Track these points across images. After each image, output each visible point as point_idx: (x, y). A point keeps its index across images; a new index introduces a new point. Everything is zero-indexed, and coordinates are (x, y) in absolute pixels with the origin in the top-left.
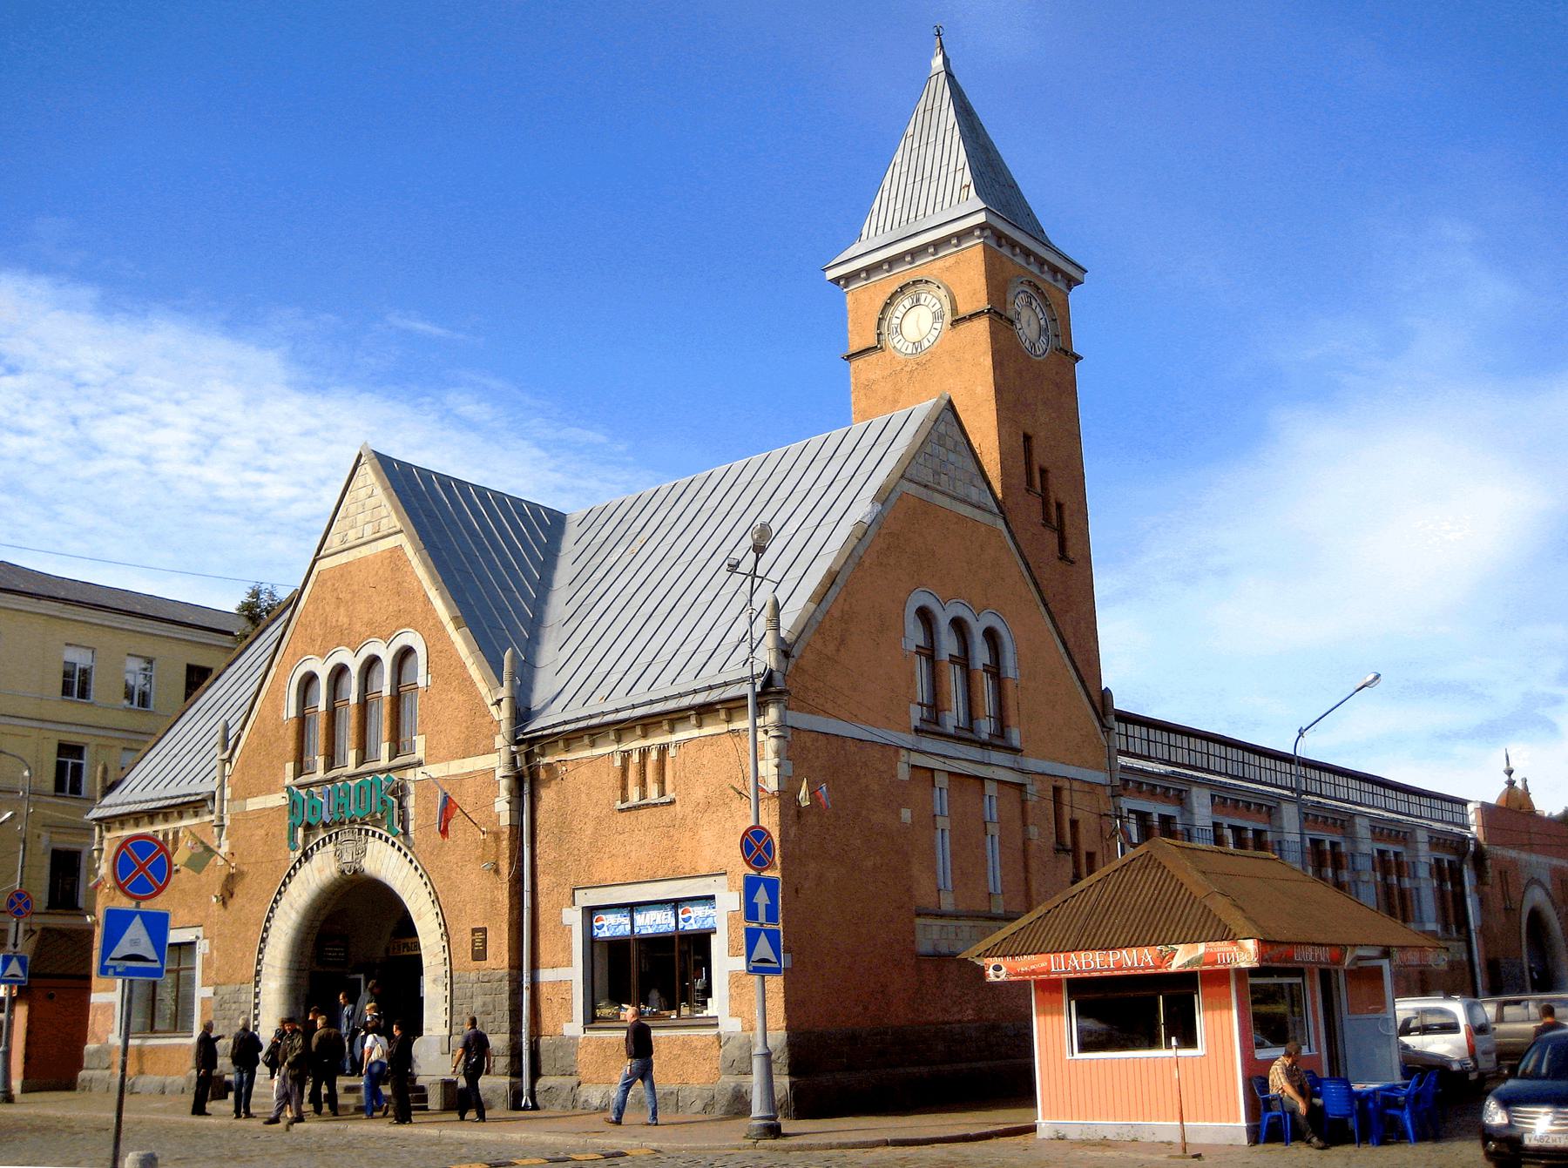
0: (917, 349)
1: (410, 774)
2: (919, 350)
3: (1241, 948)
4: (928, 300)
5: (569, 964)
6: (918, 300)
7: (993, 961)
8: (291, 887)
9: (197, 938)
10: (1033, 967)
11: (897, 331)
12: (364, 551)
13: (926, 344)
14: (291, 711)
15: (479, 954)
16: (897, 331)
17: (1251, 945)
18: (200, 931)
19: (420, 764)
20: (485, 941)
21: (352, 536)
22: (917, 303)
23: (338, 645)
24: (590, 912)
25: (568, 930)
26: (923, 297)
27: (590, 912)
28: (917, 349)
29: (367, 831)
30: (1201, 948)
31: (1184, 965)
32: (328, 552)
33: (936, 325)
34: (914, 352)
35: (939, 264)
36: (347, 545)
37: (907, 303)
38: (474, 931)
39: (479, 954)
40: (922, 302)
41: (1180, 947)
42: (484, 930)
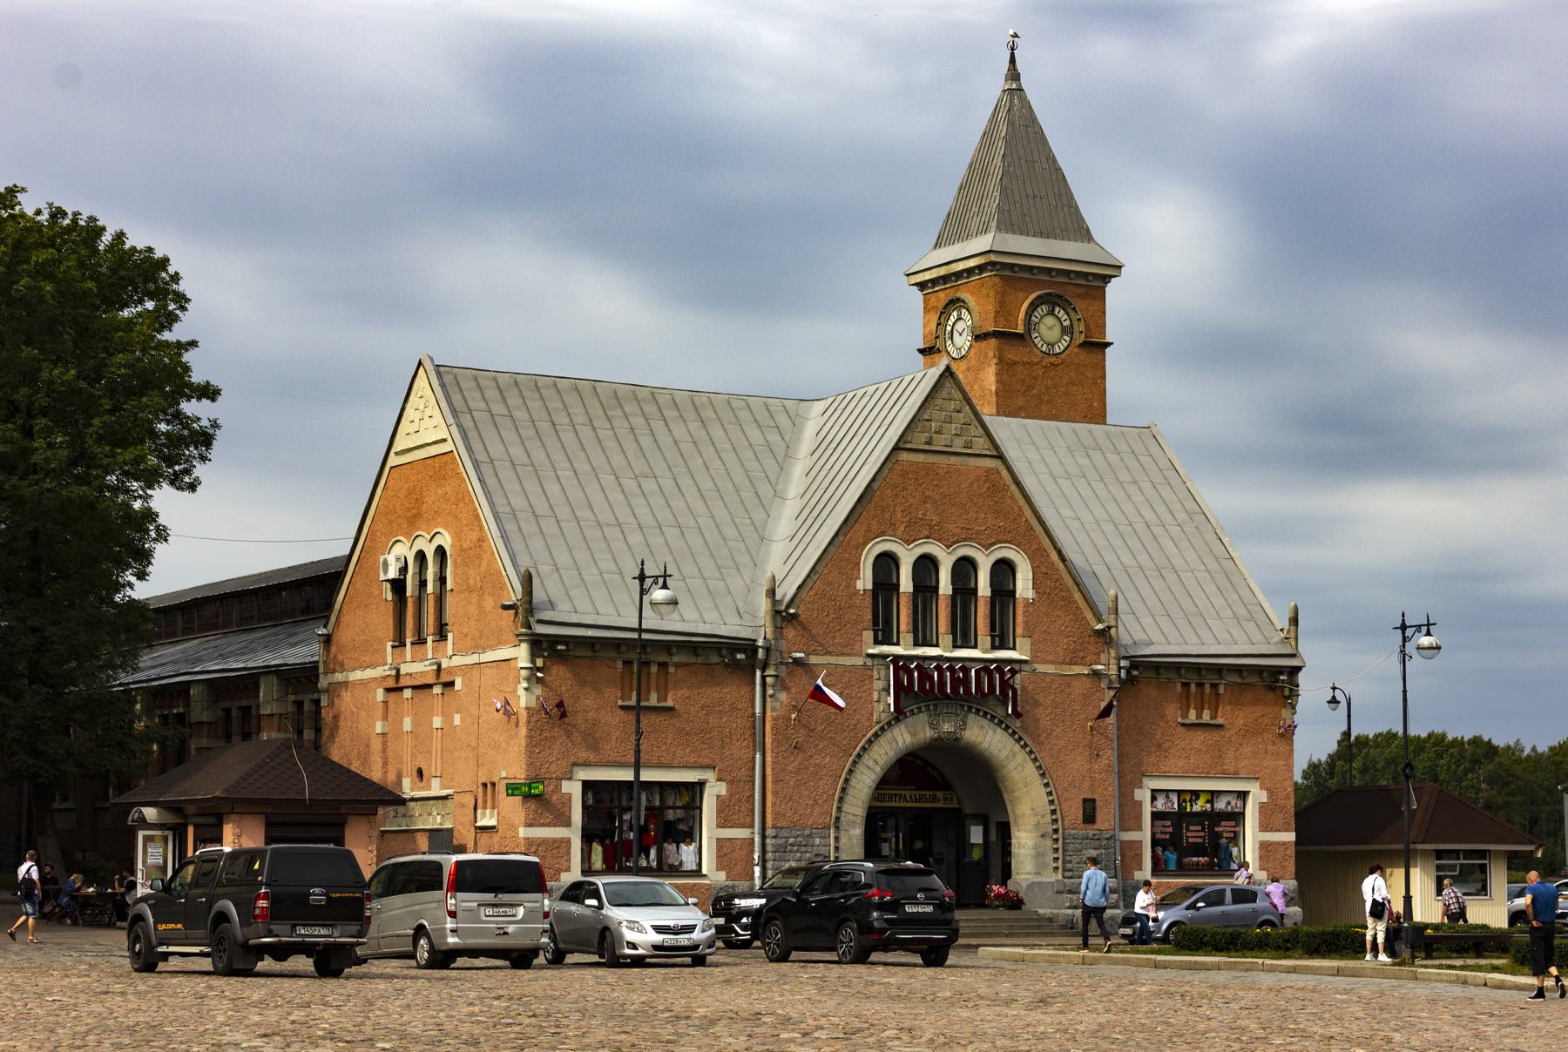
5: (1139, 828)
6: (1053, 310)
8: (875, 747)
12: (953, 459)
14: (865, 581)
15: (1089, 817)
18: (709, 776)
20: (1094, 809)
21: (940, 443)
22: (1051, 313)
23: (927, 537)
24: (1155, 794)
25: (1139, 804)
26: (1057, 309)
27: (1155, 794)
29: (970, 708)
32: (909, 446)
35: (1073, 289)
36: (932, 448)
38: (1085, 801)
39: (1089, 817)
42: (1093, 801)
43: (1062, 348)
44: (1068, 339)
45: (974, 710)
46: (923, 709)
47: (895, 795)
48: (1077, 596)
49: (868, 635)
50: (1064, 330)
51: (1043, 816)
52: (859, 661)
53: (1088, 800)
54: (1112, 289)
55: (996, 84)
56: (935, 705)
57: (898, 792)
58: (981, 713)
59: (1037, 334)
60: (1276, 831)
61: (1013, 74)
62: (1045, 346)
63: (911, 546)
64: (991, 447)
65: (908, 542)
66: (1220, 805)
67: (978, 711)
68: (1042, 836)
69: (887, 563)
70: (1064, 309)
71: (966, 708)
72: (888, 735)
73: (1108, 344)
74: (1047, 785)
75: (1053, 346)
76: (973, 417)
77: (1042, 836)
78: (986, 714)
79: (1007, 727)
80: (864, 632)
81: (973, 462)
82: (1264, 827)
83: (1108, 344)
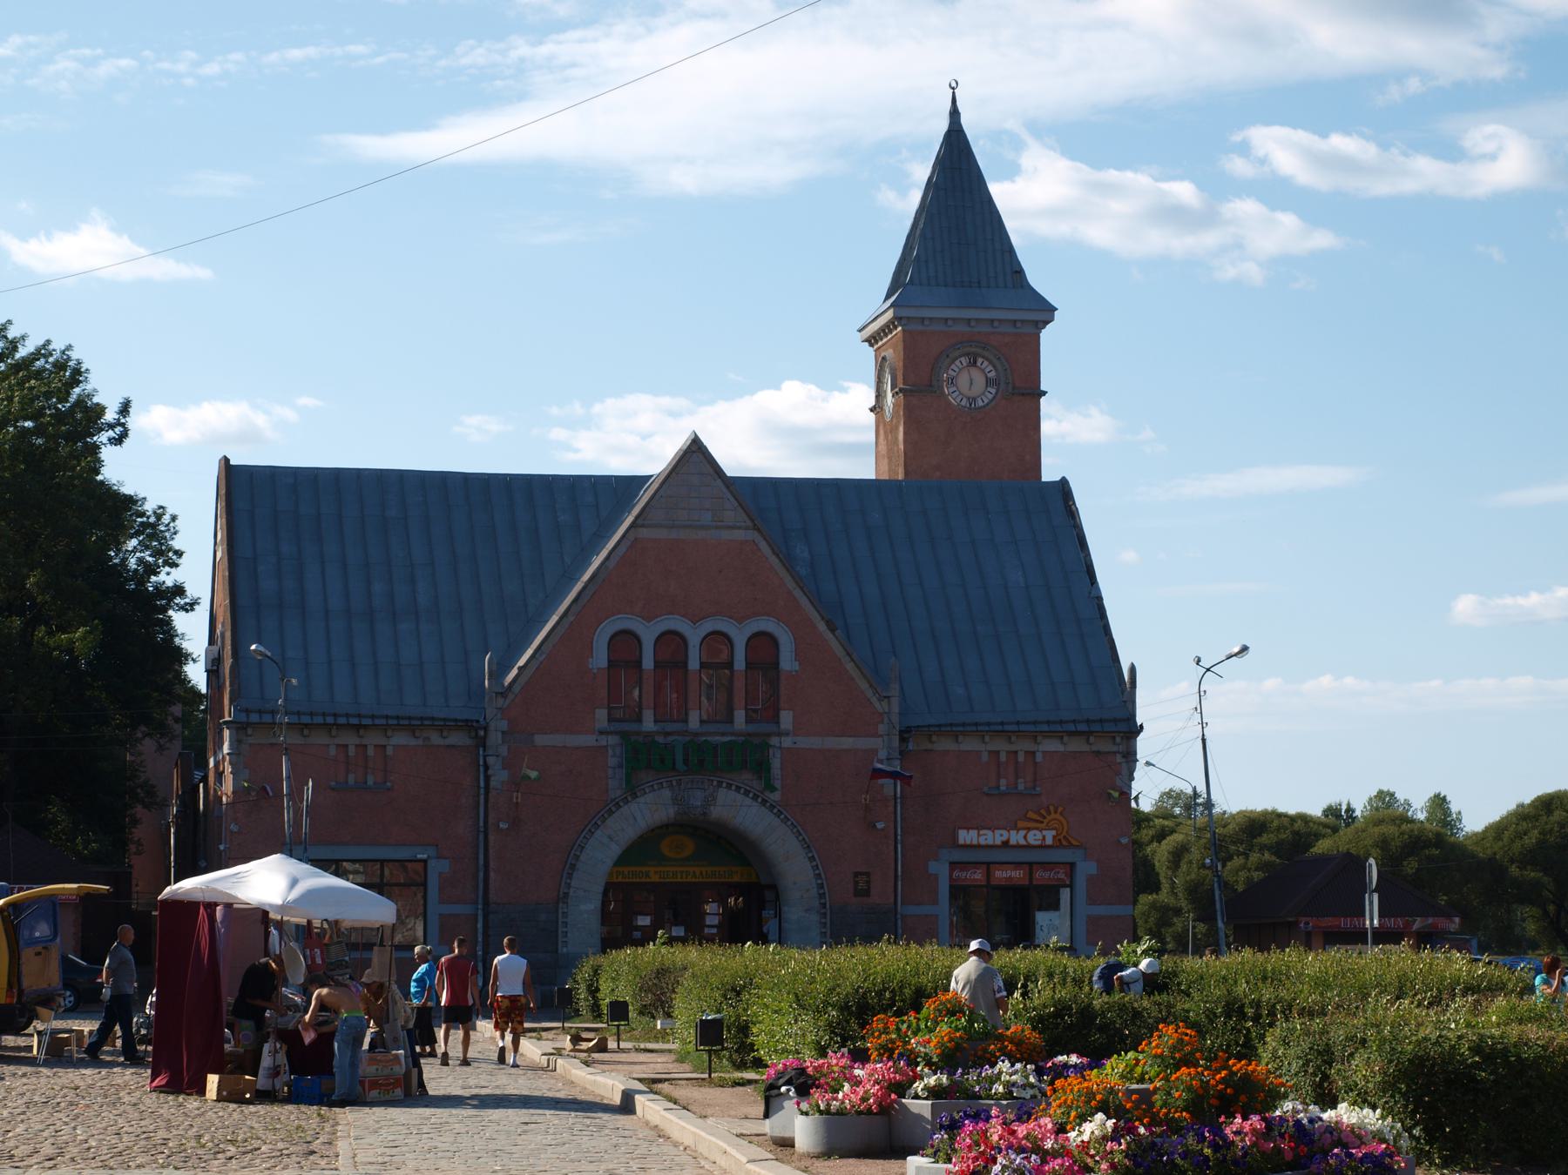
0: (970, 405)
1: (774, 741)
2: (973, 405)
3: (1454, 923)
4: (983, 366)
5: (935, 902)
6: (975, 362)
7: (1304, 920)
8: (609, 822)
9: (429, 856)
10: (1330, 924)
11: (952, 383)
13: (980, 403)
14: (600, 658)
16: (952, 383)
17: (1457, 920)
19: (787, 734)
20: (868, 882)
25: (936, 877)
26: (980, 361)
28: (970, 405)
30: (1430, 920)
31: (1419, 929)
33: (989, 389)
34: (968, 405)
37: (964, 360)
38: (856, 874)
40: (979, 364)
41: (1419, 919)
42: (868, 874)
43: (986, 401)
44: (993, 391)
45: (724, 785)
46: (665, 785)
47: (682, 872)
48: (850, 666)
49: (602, 715)
50: (989, 382)
51: (808, 890)
52: (588, 740)
53: (861, 874)
54: (1046, 335)
55: (943, 125)
56: (679, 783)
57: (685, 869)
58: (733, 788)
59: (955, 389)
60: (1109, 904)
61: (955, 113)
62: (965, 400)
63: (652, 623)
64: (746, 518)
65: (649, 619)
66: (1041, 876)
67: (729, 786)
68: (807, 911)
69: (625, 642)
70: (987, 359)
71: (715, 783)
72: (625, 809)
73: (1044, 393)
74: (812, 859)
75: (974, 399)
76: (725, 490)
77: (807, 911)
78: (738, 789)
79: (764, 802)
80: (597, 710)
81: (726, 535)
82: (1092, 901)
83: (1044, 393)
